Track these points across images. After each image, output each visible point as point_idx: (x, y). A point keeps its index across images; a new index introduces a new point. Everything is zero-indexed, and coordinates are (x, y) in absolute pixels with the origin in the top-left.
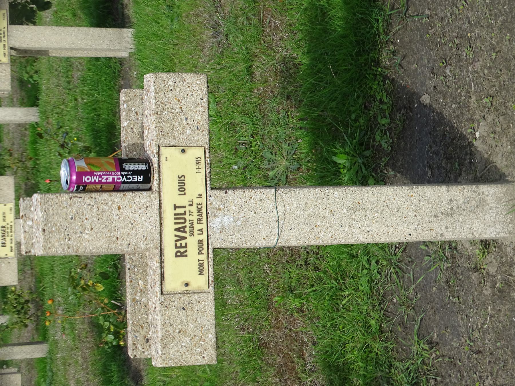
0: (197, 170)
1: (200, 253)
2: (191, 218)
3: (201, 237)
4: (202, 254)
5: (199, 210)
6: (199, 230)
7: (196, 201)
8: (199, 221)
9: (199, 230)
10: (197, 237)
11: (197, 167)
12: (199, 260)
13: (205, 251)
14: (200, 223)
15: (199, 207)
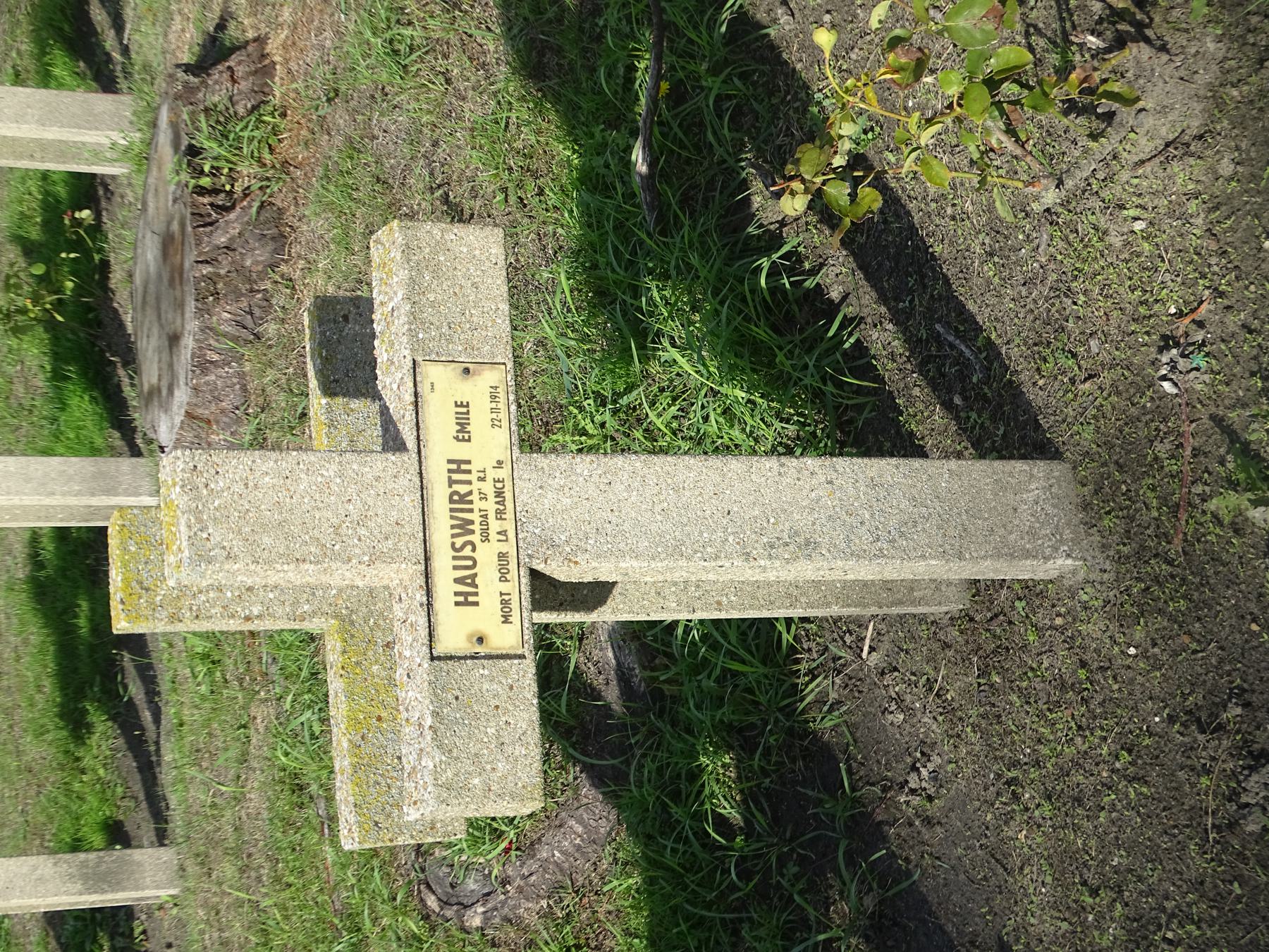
0: (494, 416)
1: (503, 579)
2: (483, 505)
3: (504, 548)
4: (507, 580)
5: (499, 494)
6: (499, 533)
7: (491, 474)
8: (500, 514)
9: (499, 533)
10: (495, 547)
11: (494, 405)
12: (501, 594)
13: (513, 574)
14: (501, 519)
15: (499, 485)
